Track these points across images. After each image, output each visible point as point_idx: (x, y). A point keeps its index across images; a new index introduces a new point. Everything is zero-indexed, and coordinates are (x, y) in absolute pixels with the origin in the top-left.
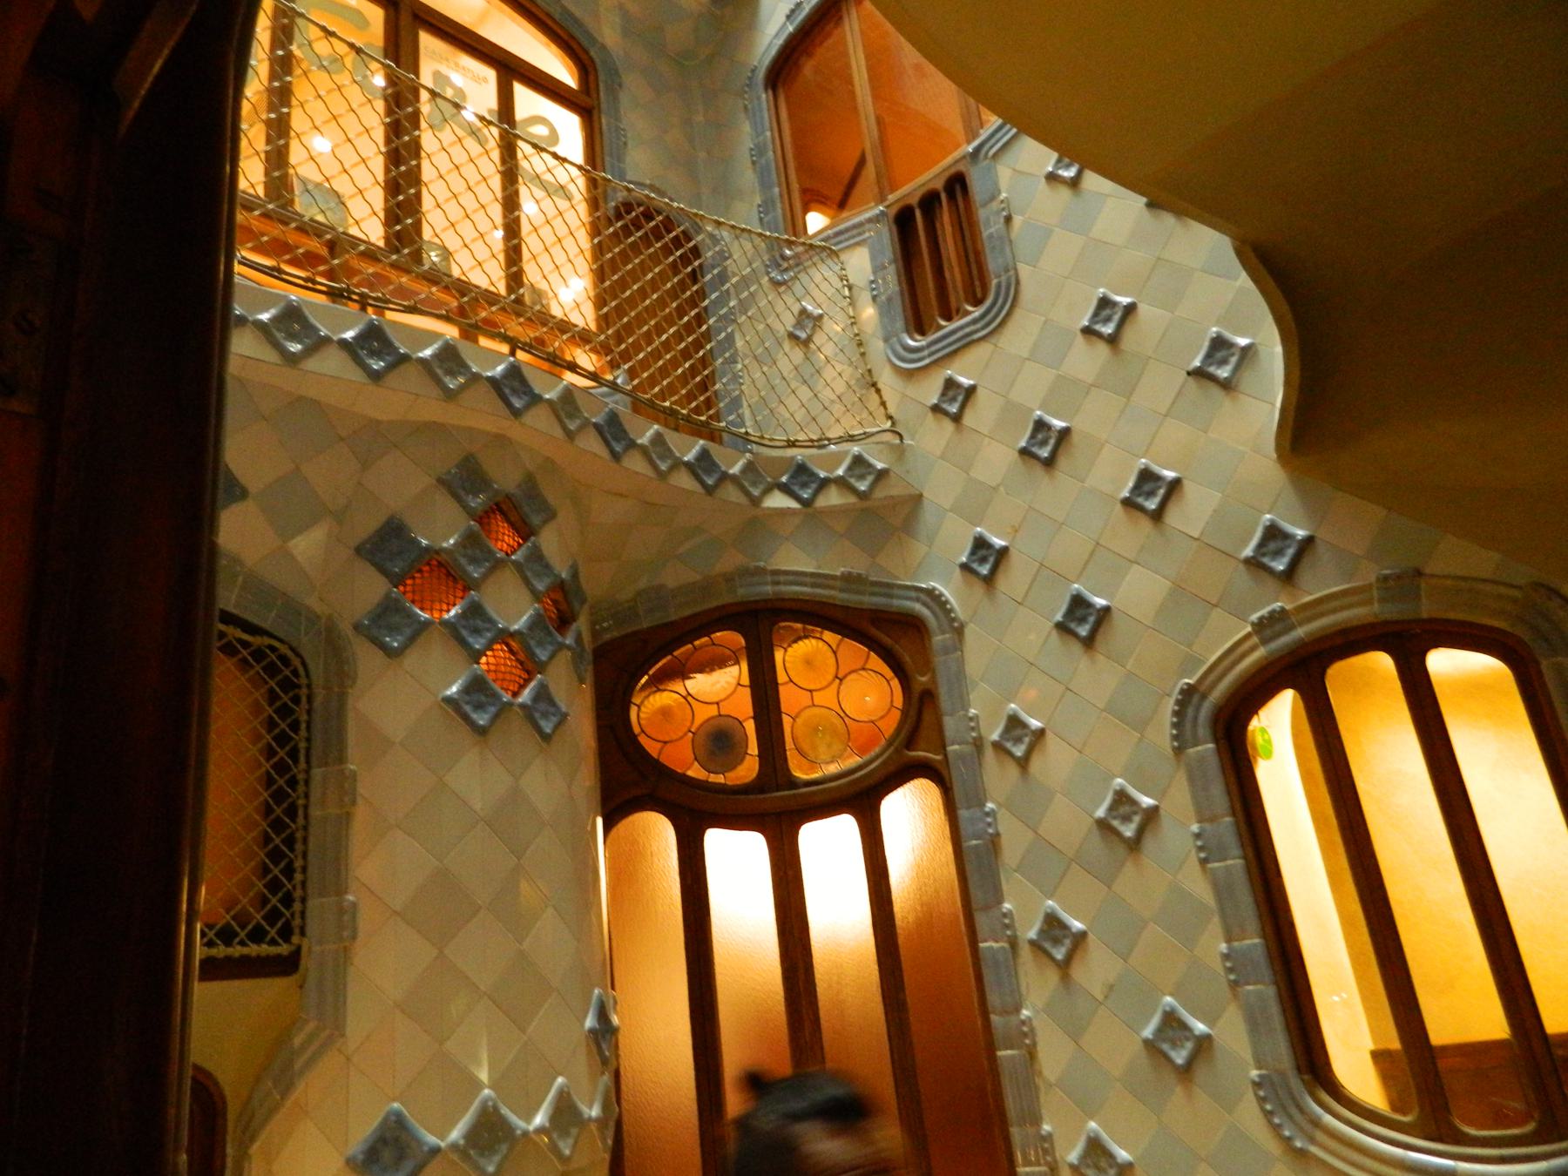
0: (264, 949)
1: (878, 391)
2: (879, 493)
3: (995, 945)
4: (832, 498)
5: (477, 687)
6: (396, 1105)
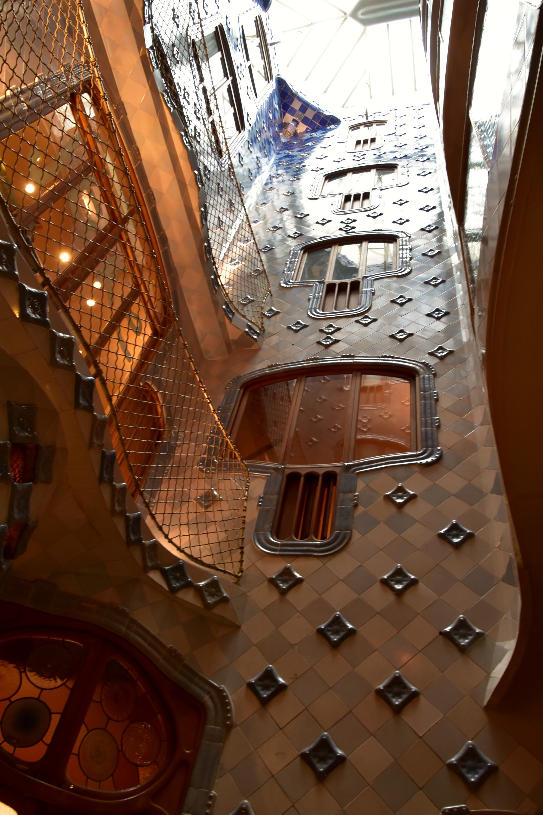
1: (242, 553)
2: (217, 611)
4: (188, 596)
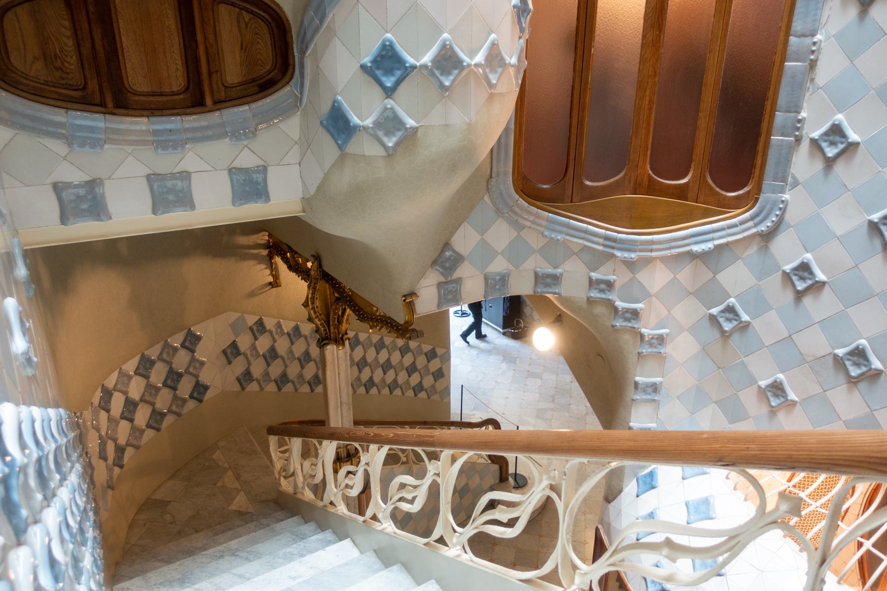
6: (389, 35)
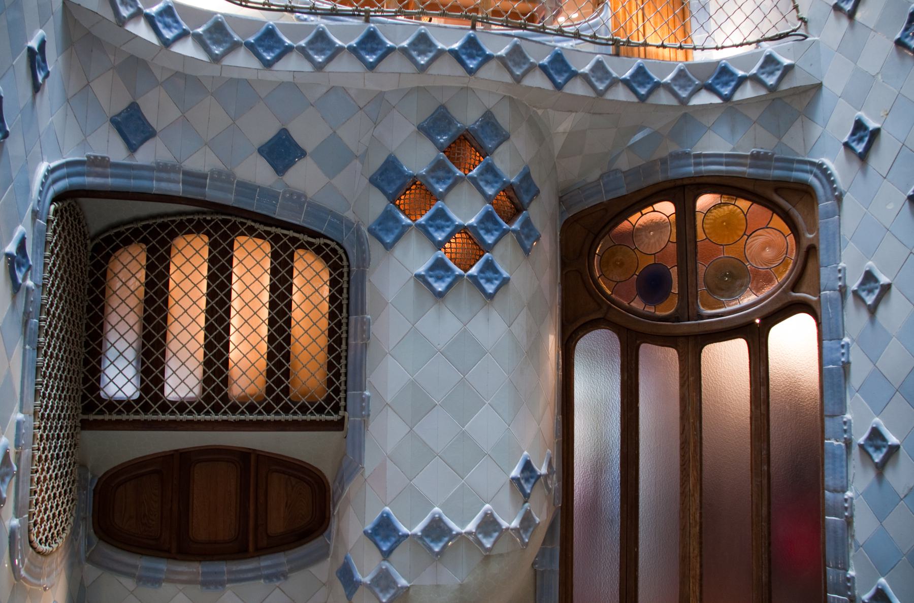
0: (324, 417)
2: (784, 86)
3: (836, 443)
4: (748, 92)
5: (439, 266)
6: (387, 509)
